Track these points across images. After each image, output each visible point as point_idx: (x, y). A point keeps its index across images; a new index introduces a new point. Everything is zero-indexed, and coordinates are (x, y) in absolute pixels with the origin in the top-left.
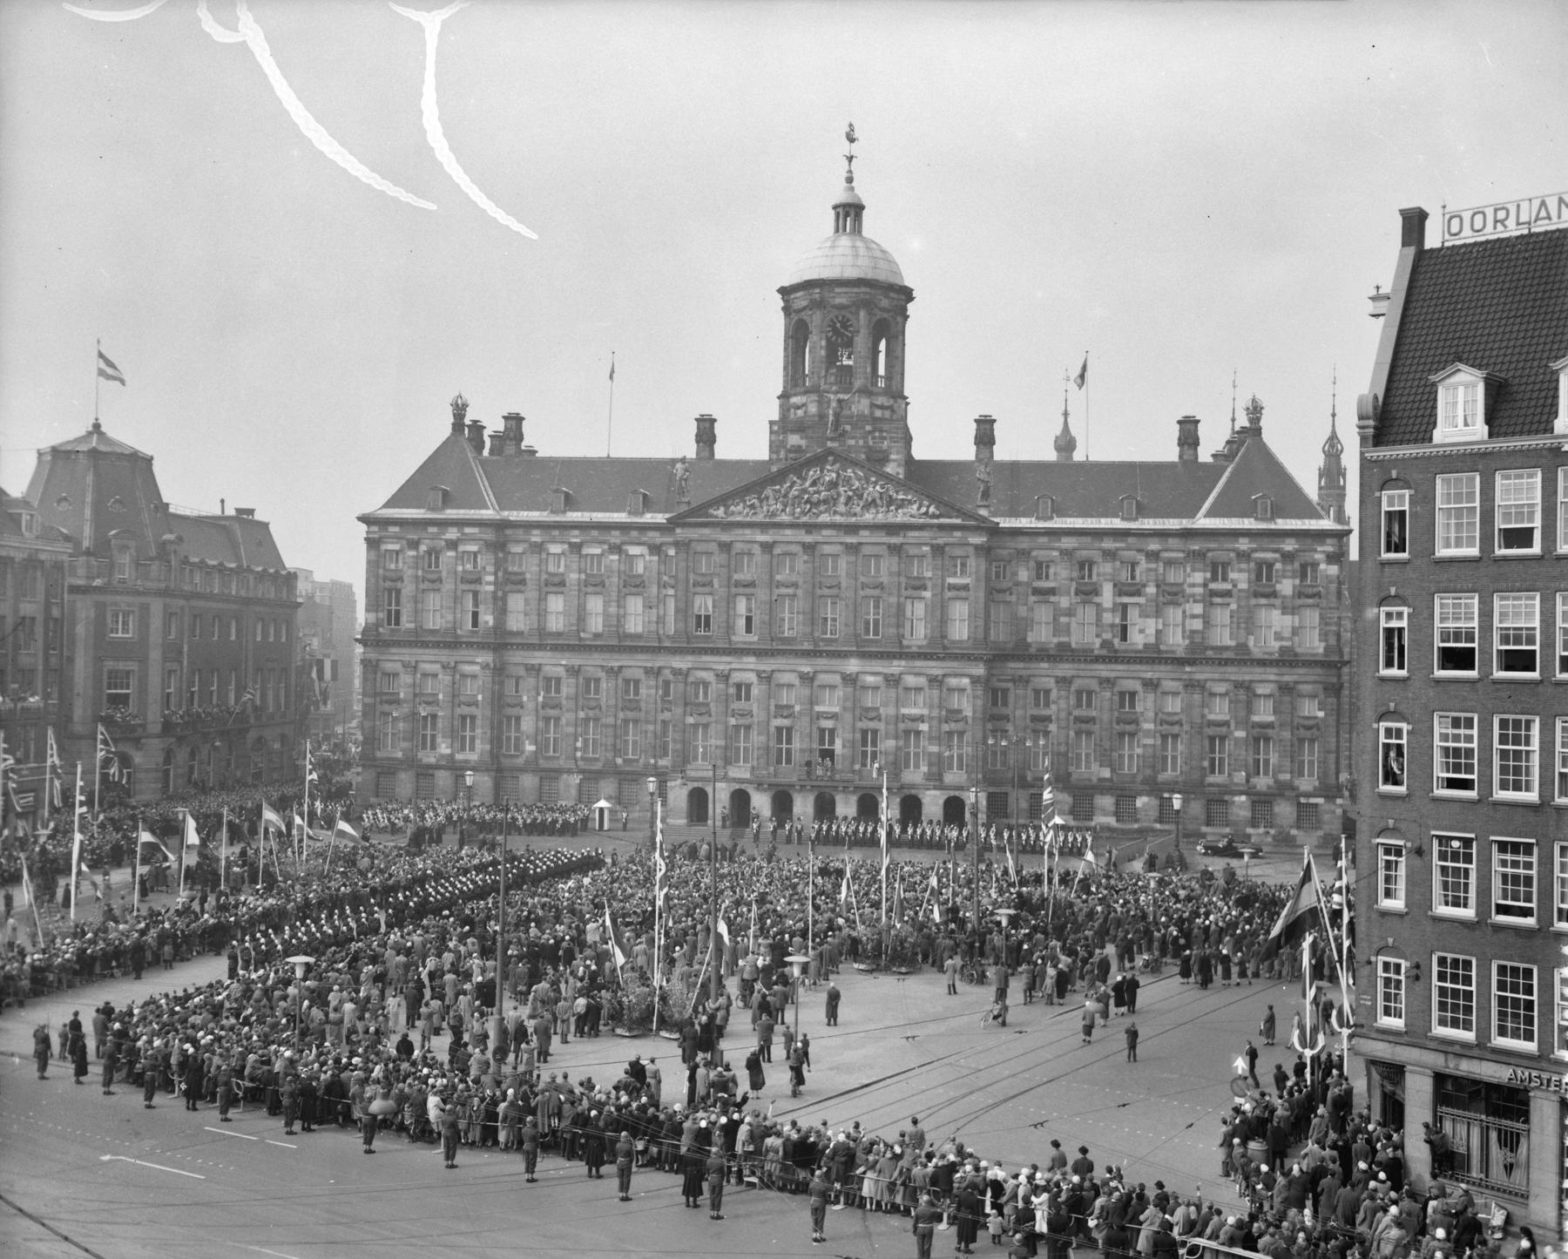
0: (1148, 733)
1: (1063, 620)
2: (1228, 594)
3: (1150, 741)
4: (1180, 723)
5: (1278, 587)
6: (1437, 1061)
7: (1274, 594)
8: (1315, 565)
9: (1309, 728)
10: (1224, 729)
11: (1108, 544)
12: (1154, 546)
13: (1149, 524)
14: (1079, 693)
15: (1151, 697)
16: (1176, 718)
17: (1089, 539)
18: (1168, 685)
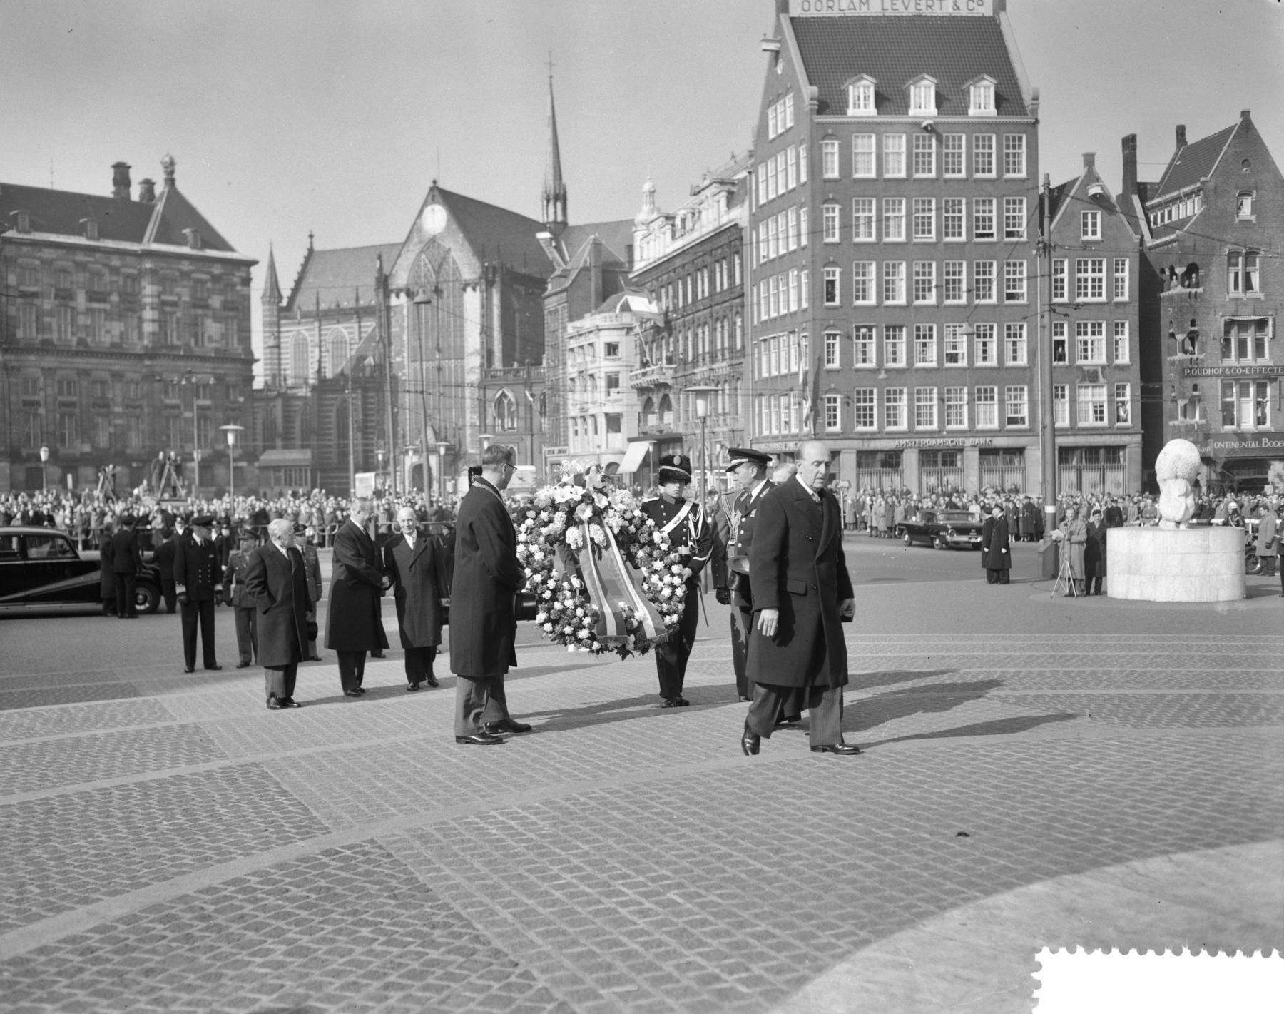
0: (118, 415)
1: (46, 319)
2: (174, 304)
3: (119, 422)
4: (140, 407)
5: (210, 301)
6: (859, 445)
7: (206, 307)
8: (234, 285)
9: (234, 410)
10: (176, 412)
11: (80, 257)
12: (116, 262)
13: (110, 244)
14: (61, 383)
15: (118, 386)
16: (137, 403)
17: (61, 252)
18: (130, 375)
